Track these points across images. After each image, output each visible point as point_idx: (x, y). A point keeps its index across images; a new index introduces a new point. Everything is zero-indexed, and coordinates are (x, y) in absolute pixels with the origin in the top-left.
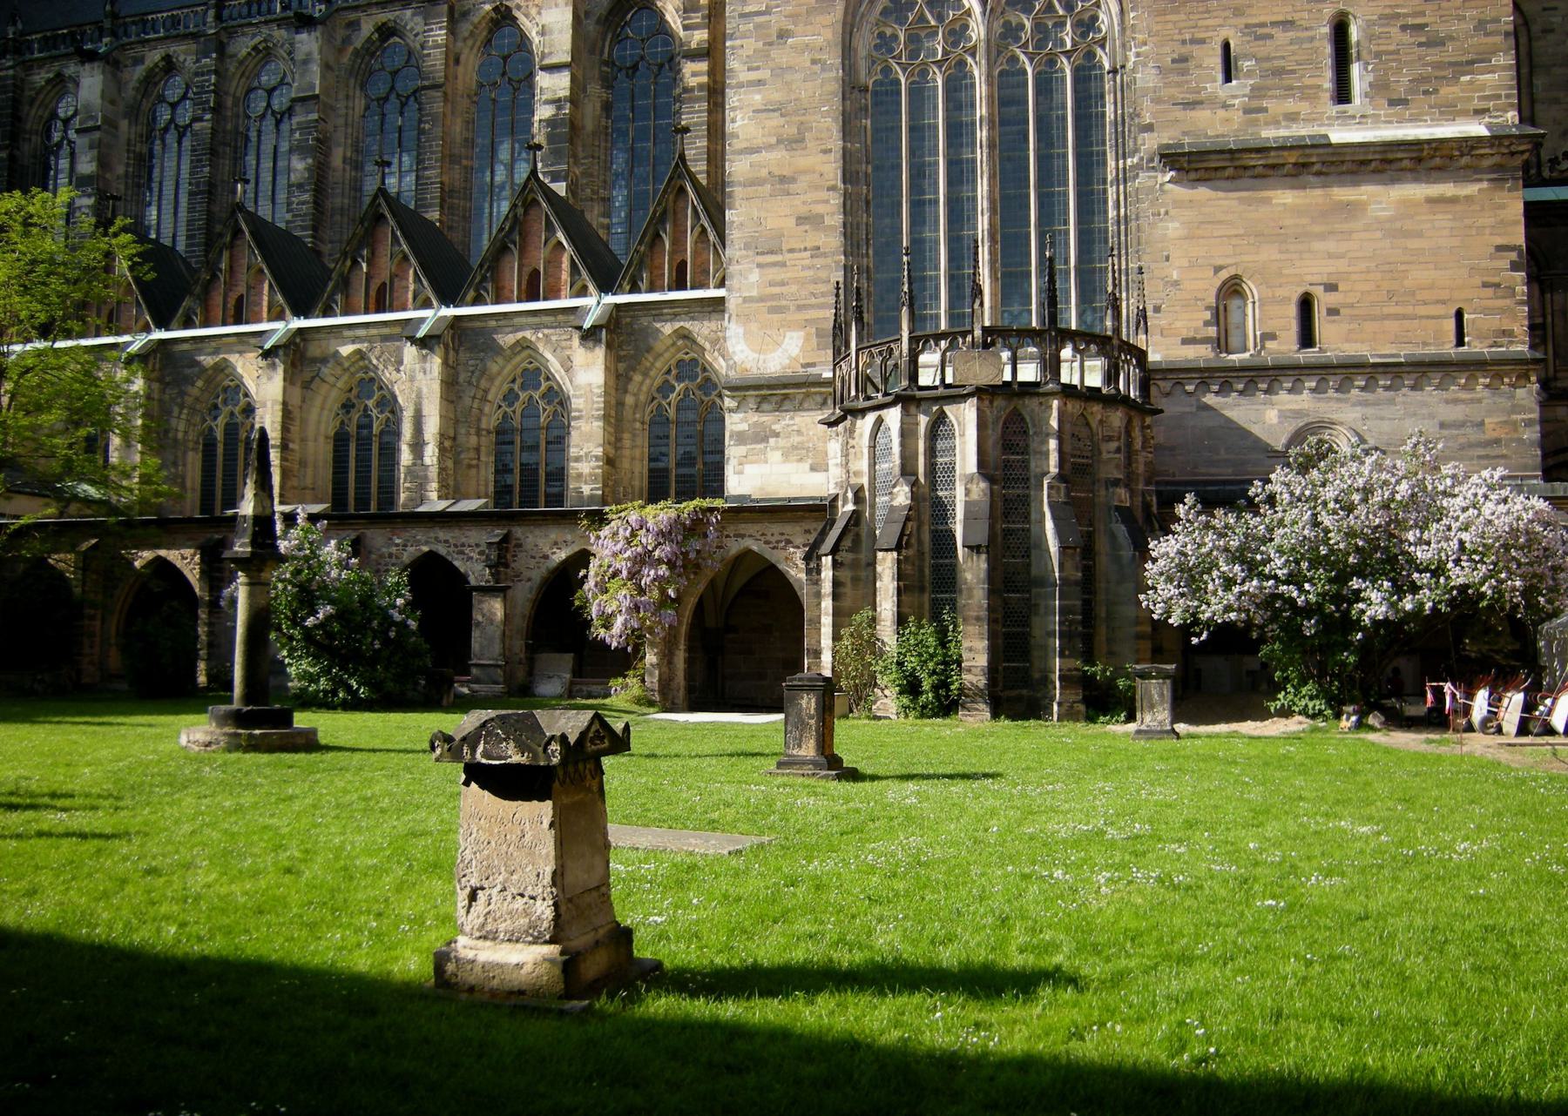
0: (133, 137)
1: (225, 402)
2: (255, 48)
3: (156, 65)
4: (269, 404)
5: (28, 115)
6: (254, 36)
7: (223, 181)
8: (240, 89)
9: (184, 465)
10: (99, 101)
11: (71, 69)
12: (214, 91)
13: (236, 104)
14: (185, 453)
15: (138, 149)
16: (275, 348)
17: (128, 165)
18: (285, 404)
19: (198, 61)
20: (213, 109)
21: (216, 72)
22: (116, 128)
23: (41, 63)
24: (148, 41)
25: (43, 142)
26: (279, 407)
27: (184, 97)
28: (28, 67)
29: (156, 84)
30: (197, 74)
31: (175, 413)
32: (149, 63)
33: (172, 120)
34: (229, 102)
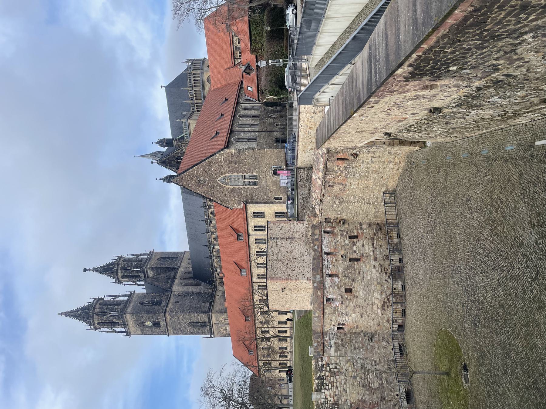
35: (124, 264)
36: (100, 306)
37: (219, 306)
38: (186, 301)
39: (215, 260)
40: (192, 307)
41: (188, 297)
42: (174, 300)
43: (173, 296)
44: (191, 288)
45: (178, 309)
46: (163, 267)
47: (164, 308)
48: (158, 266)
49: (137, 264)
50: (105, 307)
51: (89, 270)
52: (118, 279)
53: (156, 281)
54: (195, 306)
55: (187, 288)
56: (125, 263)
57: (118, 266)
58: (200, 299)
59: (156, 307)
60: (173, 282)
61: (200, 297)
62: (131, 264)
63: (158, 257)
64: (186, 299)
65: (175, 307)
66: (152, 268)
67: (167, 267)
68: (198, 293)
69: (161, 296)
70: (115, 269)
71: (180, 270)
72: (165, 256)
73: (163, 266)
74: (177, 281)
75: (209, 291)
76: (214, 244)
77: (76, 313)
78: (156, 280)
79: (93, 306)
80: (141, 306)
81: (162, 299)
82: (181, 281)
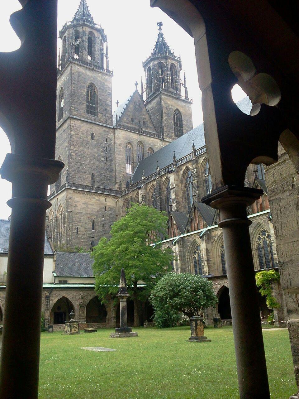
0: (182, 187)
1: (197, 250)
2: (204, 160)
3: (185, 169)
4: (203, 249)
5: (163, 188)
6: (203, 157)
7: (201, 193)
8: (202, 170)
9: (190, 267)
10: (174, 181)
11: (169, 175)
12: (196, 173)
13: (202, 174)
14: (190, 264)
15: (184, 190)
16: (203, 235)
17: (182, 194)
18: (207, 249)
19: (192, 166)
20: (197, 177)
21: (196, 168)
22: (179, 186)
23: (163, 175)
24: (182, 164)
25: (166, 193)
26: (205, 250)
27: (191, 176)
28: (161, 177)
29: (186, 174)
30: (192, 170)
31: (187, 255)
32: (183, 170)
33: (190, 181)
34: (200, 174)
37: (83, 201)
39: (155, 183)
44: (121, 157)
46: (162, 117)
49: (167, 82)
50: (85, 38)
51: (160, 29)
57: (163, 58)
59: (84, 106)
60: (133, 130)
62: (168, 74)
66: (161, 102)
67: (162, 122)
68: (111, 169)
70: (158, 56)
72: (183, 119)
73: (165, 118)
74: (135, 137)
75: (117, 186)
76: (177, 172)
77: (82, 10)
78: (137, 107)
79: (86, 23)
81: (100, 114)
82: (135, 143)
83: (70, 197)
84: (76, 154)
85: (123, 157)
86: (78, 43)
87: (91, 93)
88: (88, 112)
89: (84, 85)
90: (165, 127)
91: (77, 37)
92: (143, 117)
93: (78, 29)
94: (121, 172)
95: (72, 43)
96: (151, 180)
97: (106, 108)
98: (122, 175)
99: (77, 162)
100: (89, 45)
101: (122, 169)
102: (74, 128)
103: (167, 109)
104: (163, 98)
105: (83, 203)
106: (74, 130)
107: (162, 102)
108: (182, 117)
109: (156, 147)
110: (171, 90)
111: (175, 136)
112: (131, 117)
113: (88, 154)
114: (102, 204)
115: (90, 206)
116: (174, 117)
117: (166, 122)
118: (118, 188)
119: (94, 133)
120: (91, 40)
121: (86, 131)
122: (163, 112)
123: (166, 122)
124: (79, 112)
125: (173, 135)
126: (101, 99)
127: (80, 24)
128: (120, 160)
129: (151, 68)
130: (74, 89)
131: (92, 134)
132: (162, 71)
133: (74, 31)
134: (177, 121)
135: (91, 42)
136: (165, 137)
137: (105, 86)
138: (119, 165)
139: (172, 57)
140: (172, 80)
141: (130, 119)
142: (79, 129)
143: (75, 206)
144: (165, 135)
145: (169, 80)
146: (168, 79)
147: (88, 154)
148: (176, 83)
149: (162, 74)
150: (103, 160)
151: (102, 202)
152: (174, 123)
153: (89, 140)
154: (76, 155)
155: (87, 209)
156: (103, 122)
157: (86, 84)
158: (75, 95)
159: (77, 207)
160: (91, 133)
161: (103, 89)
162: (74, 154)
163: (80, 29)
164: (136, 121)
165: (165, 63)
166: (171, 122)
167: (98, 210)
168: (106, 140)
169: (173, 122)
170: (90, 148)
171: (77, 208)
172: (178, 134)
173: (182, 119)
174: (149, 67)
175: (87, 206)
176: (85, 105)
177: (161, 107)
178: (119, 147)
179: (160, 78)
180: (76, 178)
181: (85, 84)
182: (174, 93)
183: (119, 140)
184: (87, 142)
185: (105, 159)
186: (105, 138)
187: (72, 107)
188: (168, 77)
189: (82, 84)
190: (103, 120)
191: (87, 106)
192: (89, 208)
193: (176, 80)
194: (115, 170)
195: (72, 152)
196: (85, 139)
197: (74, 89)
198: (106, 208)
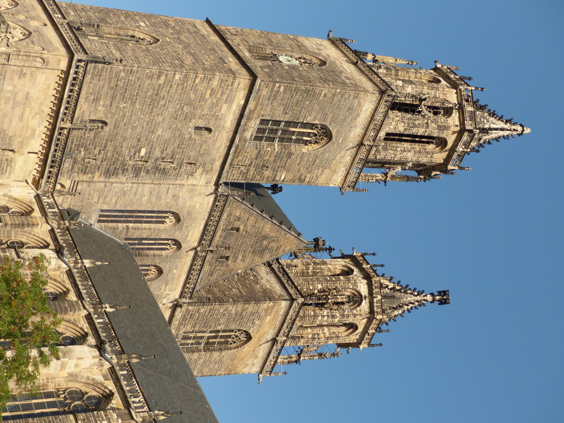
35: (355, 316)
36: (444, 136)
38: (167, 135)
40: (148, 101)
41: (157, 153)
42: (214, 143)
43: (213, 161)
44: (145, 199)
45: (202, 98)
47: (251, 105)
48: (251, 307)
49: (315, 316)
52: (358, 265)
53: (265, 237)
54: (133, 104)
55: (159, 198)
56: (350, 320)
58: (112, 138)
61: (110, 148)
62: (333, 317)
63: (247, 347)
64: (167, 143)
65: (213, 106)
67: (221, 301)
68: (115, 173)
69: (256, 167)
71: (176, 294)
72: (224, 353)
73: (232, 309)
75: (67, 183)
77: (493, 126)
78: (265, 243)
79: (466, 134)
80: (327, 124)
82: (178, 236)
83: (48, 62)
84: (163, 87)
85: (145, 203)
86: (425, 111)
87: (308, 135)
88: (264, 122)
89: (329, 120)
90: (208, 310)
91: (435, 110)
92: (240, 257)
93: (453, 115)
94: (106, 197)
95: (425, 99)
96: (80, 287)
97: (269, 169)
98: (96, 199)
99: (140, 86)
100: (416, 136)
101: (111, 199)
102: (228, 85)
103: (252, 314)
104: (280, 305)
105: (28, 93)
106: (223, 85)
107: (271, 304)
108: (231, 349)
109: (163, 287)
110: (298, 323)
111: (184, 333)
112: (242, 228)
113: (158, 114)
114: (22, 145)
115: (18, 111)
116: (232, 331)
117: (221, 311)
118: (63, 186)
119: (211, 135)
120: (428, 143)
121: (218, 116)
122: (247, 306)
123: (221, 311)
124: (266, 102)
125: (189, 328)
126: (293, 157)
127: (464, 120)
128: (135, 195)
129: (350, 276)
130: (323, 95)
131: (209, 130)
132: (343, 303)
133: (451, 105)
134: (222, 337)
135: (423, 142)
136: (185, 307)
137: (321, 170)
138: (125, 191)
139: (370, 328)
140: (320, 326)
141: (237, 224)
142: (224, 97)
143: (22, 71)
144: (190, 308)
145: (320, 318)
146: (323, 316)
147: (158, 114)
148: (310, 336)
149: (337, 303)
150: (139, 151)
151: (28, 142)
152: (218, 331)
153: (193, 121)
154: (160, 84)
155: (11, 103)
156: (237, 157)
157: (330, 124)
158: (307, 96)
159: (20, 78)
160: (212, 128)
161: (313, 165)
162: (161, 81)
163: (455, 119)
164: (231, 242)
165: (360, 310)
166: (220, 324)
167: (7, 132)
168: (191, 164)
169: (219, 328)
170: (174, 123)
171: (16, 78)
172: (189, 338)
173: (225, 349)
174: (352, 271)
175: (18, 102)
176: (282, 119)
177: (258, 301)
178: (170, 195)
179: (327, 299)
180: (99, 80)
181: (331, 121)
182: (289, 332)
183: (188, 196)
184: (188, 118)
185: (142, 157)
186: (196, 162)
187: (280, 87)
188: (328, 316)
189: (331, 115)
190: (240, 158)
191: (278, 123)
192: (13, 108)
193: (318, 334)
194: (111, 180)
195: (167, 75)
196: (199, 111)
197: (323, 95)
198: (11, 153)
